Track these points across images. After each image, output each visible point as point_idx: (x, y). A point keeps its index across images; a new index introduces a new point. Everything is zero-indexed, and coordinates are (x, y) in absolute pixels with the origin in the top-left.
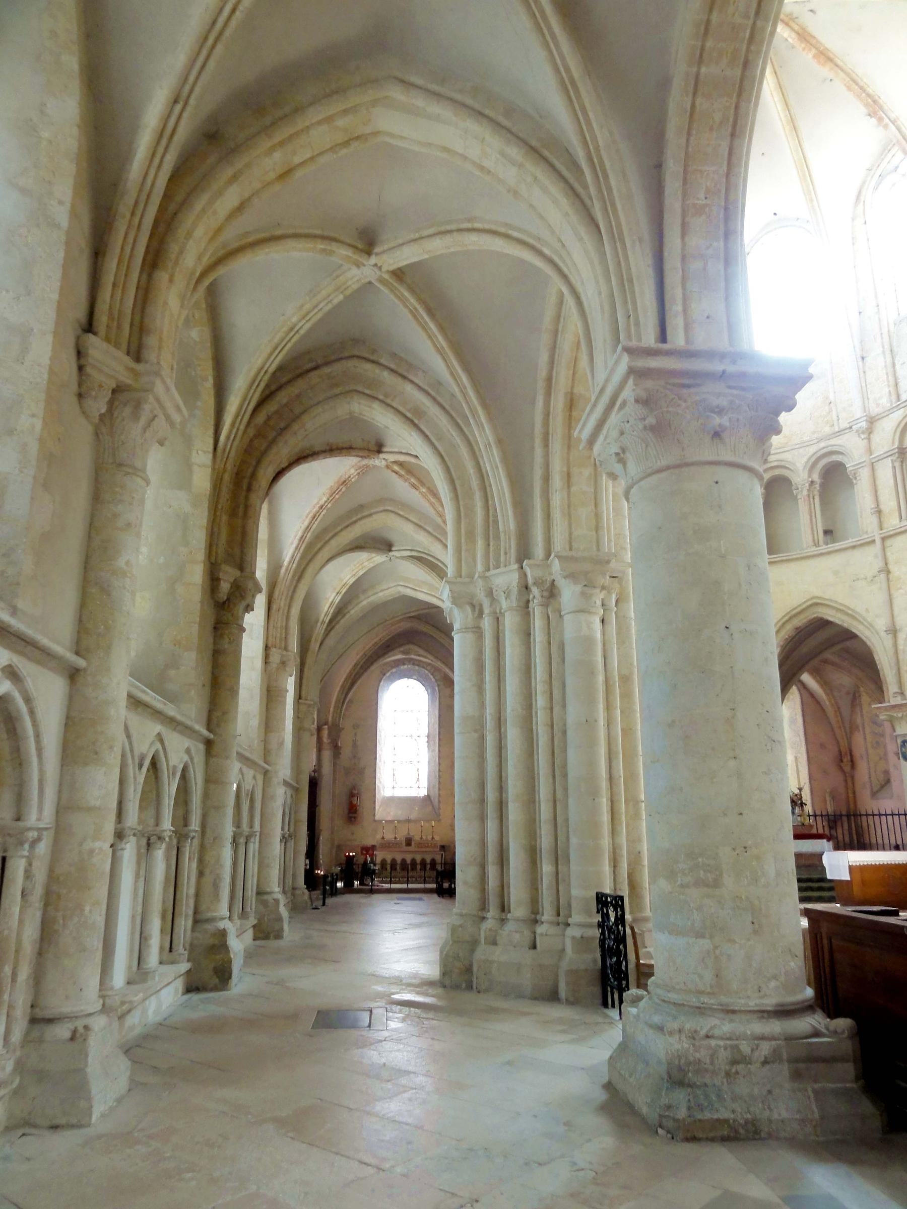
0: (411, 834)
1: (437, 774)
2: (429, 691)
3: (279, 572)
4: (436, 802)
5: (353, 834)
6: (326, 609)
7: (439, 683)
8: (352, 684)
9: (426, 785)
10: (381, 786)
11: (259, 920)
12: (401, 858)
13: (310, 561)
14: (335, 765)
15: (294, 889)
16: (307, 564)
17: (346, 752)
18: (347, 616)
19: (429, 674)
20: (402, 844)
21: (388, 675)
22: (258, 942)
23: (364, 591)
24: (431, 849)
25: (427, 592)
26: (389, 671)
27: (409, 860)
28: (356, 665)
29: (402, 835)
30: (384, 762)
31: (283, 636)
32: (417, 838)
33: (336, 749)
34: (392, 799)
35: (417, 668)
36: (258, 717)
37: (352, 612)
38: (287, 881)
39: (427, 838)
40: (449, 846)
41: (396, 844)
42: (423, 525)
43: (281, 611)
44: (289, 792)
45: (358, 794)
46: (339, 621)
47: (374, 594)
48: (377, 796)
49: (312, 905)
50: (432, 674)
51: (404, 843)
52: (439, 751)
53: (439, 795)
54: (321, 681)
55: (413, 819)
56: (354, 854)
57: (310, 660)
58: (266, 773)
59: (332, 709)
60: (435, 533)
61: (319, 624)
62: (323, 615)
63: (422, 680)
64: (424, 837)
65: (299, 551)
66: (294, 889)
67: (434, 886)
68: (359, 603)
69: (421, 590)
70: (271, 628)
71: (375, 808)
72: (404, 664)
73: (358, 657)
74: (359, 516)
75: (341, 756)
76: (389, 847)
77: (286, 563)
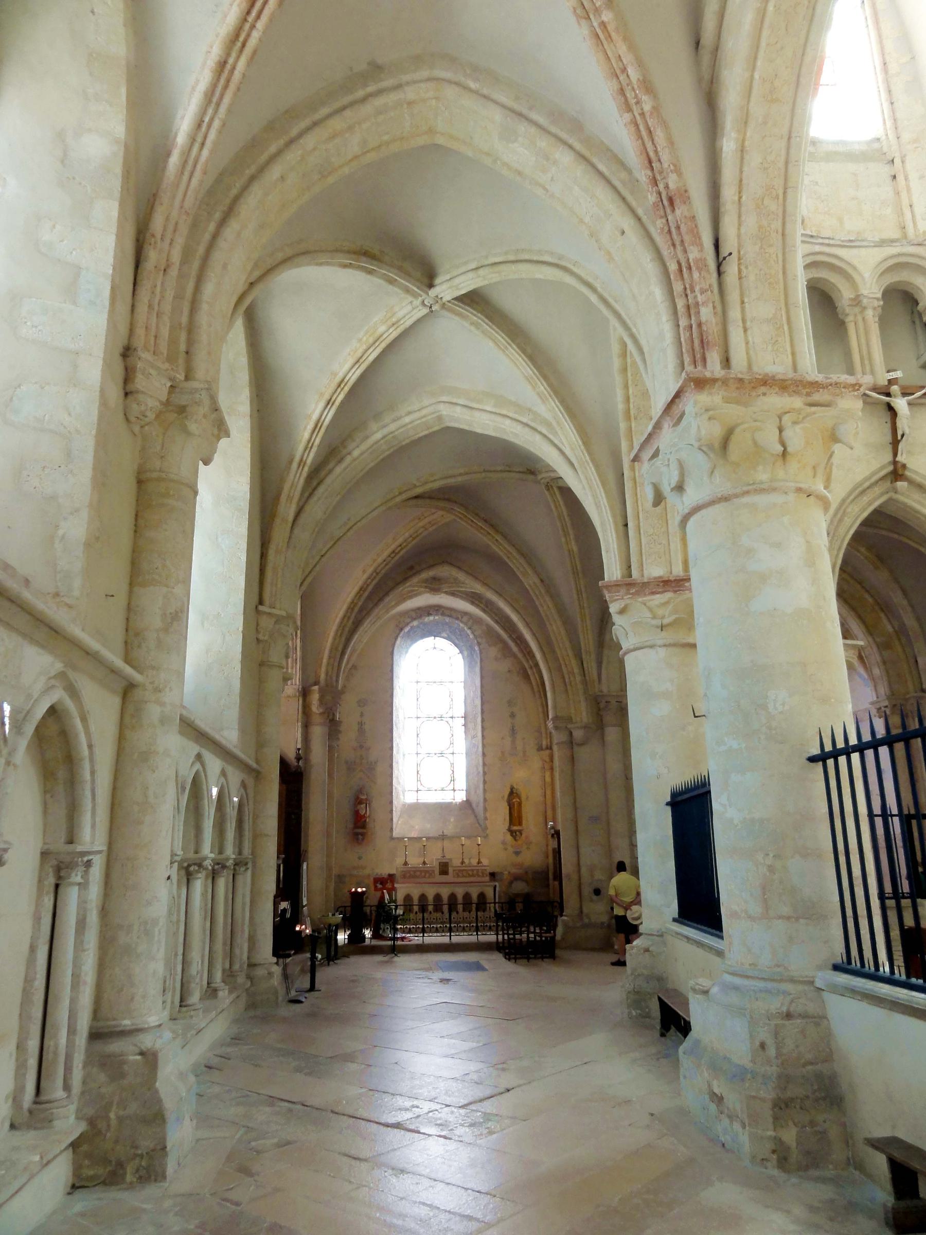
0: (448, 856)
1: (481, 769)
2: (466, 653)
3: (164, 168)
4: (480, 810)
5: (360, 858)
6: (306, 435)
7: (480, 640)
8: (357, 624)
9: (464, 787)
10: (400, 789)
11: (92, 1122)
12: (435, 893)
13: (253, 179)
14: (331, 749)
15: (252, 965)
16: (245, 188)
17: (348, 737)
18: (348, 459)
19: (466, 628)
20: (433, 871)
21: (406, 629)
22: (83, 1202)
23: (377, 416)
24: (479, 879)
25: (494, 410)
26: (408, 624)
27: (445, 893)
28: (362, 589)
29: (433, 858)
30: (404, 755)
31: (183, 347)
32: (456, 862)
33: (333, 726)
34: (416, 808)
35: (447, 619)
36: (85, 514)
37: (356, 453)
38: (237, 951)
39: (470, 863)
40: (502, 873)
41: (426, 872)
42: (525, 111)
43: (174, 272)
44: (235, 777)
45: (366, 799)
46: (330, 471)
47: (394, 421)
48: (395, 802)
49: (288, 990)
50: (470, 628)
51: (437, 872)
52: (483, 736)
53: (485, 800)
54: (301, 585)
55: (449, 835)
56: (364, 889)
57: (279, 534)
58: (128, 690)
59: (325, 661)
60: (553, 129)
61: (295, 465)
62: (301, 448)
63: (455, 638)
64: (466, 861)
65: (216, 111)
66: (252, 965)
67: (490, 937)
68: (367, 437)
69: (480, 407)
70: (142, 308)
71: (392, 819)
72: (429, 614)
73: (365, 576)
74: (371, 89)
75: (340, 736)
76: (414, 877)
77: (181, 139)
